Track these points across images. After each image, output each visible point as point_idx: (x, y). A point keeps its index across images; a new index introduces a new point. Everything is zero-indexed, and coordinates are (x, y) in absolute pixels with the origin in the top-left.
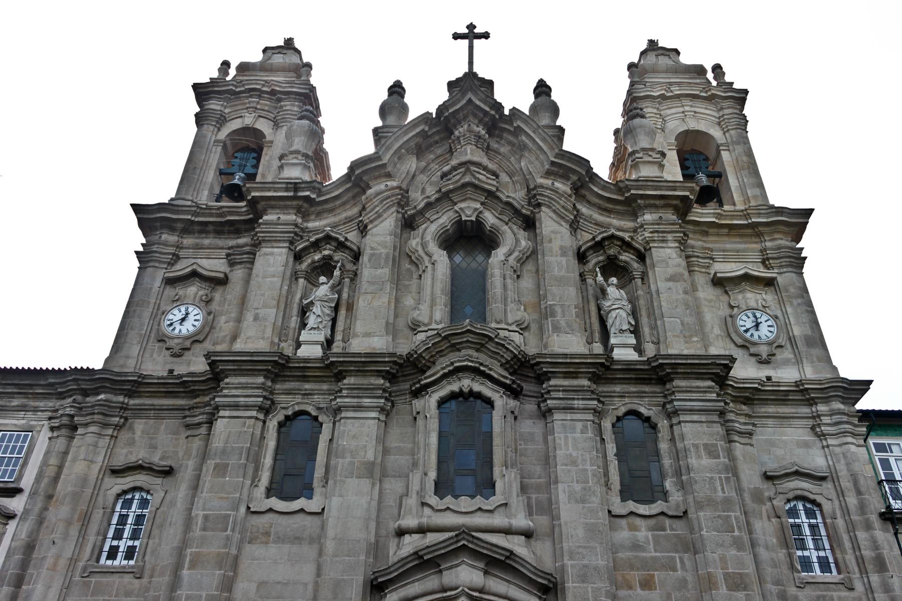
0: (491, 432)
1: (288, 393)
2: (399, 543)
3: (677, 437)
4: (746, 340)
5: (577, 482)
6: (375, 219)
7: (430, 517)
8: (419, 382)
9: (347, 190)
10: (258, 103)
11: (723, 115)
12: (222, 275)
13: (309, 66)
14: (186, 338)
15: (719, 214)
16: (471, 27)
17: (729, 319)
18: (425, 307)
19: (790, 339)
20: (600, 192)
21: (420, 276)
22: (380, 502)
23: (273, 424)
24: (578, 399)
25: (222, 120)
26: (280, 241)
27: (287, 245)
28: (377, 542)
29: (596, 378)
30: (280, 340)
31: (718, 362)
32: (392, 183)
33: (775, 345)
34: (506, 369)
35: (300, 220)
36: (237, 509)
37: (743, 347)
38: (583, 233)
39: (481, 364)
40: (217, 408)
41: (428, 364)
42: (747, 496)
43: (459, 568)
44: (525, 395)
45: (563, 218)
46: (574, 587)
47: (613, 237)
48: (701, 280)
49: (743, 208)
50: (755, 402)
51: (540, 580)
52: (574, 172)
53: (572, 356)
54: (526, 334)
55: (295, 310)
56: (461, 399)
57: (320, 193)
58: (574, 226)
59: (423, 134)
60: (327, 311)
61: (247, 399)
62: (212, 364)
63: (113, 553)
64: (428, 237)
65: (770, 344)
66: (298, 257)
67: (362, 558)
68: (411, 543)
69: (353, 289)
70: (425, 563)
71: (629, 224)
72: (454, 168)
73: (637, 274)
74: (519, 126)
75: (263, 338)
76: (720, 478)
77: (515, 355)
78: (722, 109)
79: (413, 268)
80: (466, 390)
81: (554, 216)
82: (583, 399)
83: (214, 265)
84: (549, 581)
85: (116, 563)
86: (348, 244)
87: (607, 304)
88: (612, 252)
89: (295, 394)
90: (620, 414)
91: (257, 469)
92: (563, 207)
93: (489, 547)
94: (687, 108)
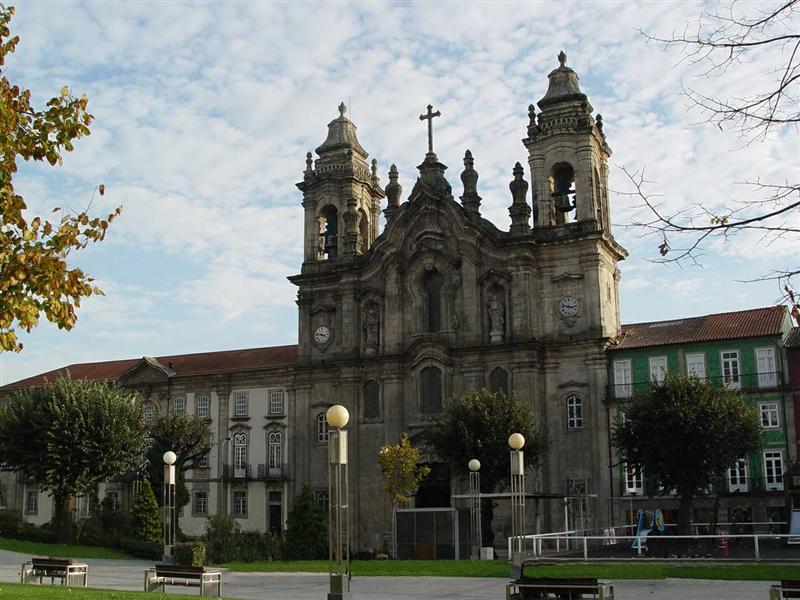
23: (361, 387)
25: (315, 203)
32: (393, 250)
48: (546, 280)
58: (479, 264)
65: (574, 316)
83: (329, 301)
94: (558, 144)
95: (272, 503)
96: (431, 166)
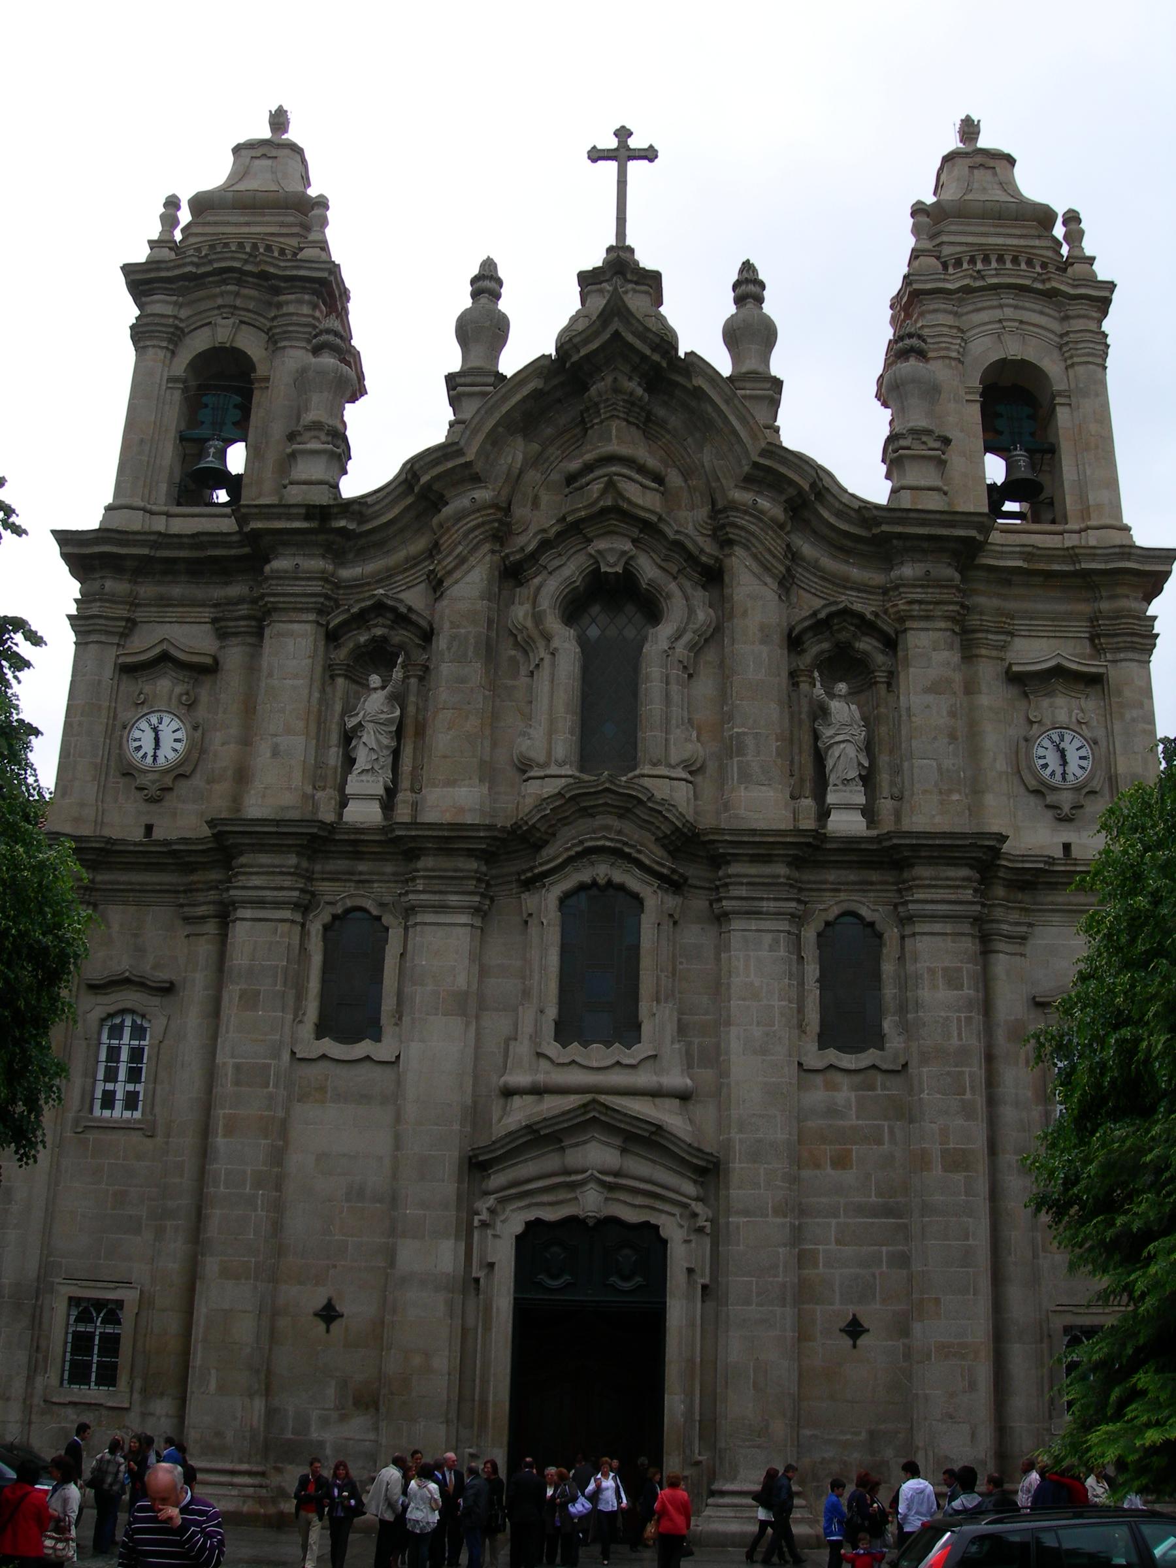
0: (636, 947)
1: (333, 878)
2: (504, 1109)
3: (907, 955)
4: (1043, 783)
5: (758, 1024)
6: (456, 568)
7: (548, 1073)
8: (531, 869)
9: (407, 509)
10: (237, 294)
11: (1067, 333)
12: (208, 661)
13: (322, 203)
14: (167, 772)
15: (1029, 553)
16: (623, 134)
17: (1023, 744)
19: (1110, 779)
20: (832, 520)
21: (532, 672)
22: (477, 1047)
23: (315, 928)
24: (768, 899)
25: (176, 336)
26: (301, 610)
27: (312, 617)
28: (475, 1103)
29: (797, 863)
30: (314, 788)
31: (980, 843)
32: (483, 495)
34: (663, 846)
35: (330, 568)
36: (277, 1056)
37: (1037, 792)
38: (801, 592)
39: (626, 844)
40: (234, 904)
41: (545, 837)
42: (1001, 1035)
43: (588, 1146)
44: (690, 886)
45: (767, 569)
46: (742, 1169)
47: (846, 612)
48: (988, 671)
49: (1076, 527)
50: (1040, 887)
51: (695, 1161)
52: (791, 482)
53: (764, 833)
54: (699, 779)
55: (334, 738)
56: (594, 892)
57: (362, 518)
58: (786, 584)
59: (536, 395)
60: (385, 741)
61: (275, 893)
62: (218, 837)
63: (108, 1100)
64: (545, 603)
65: (1077, 789)
66: (332, 637)
67: (456, 1127)
68: (521, 1112)
70: (541, 1137)
71: (876, 578)
72: (588, 468)
73: (881, 676)
74: (700, 388)
75: (289, 789)
76: (959, 1019)
77: (677, 828)
78: (1066, 318)
79: (519, 656)
80: (601, 881)
81: (755, 566)
82: (775, 899)
83: (192, 637)
84: (708, 1161)
85: (117, 1113)
86: (414, 617)
87: (828, 732)
88: (843, 636)
89: (345, 881)
90: (831, 917)
91: (300, 997)
92: (769, 551)
93: (628, 1120)
94: (1009, 312)
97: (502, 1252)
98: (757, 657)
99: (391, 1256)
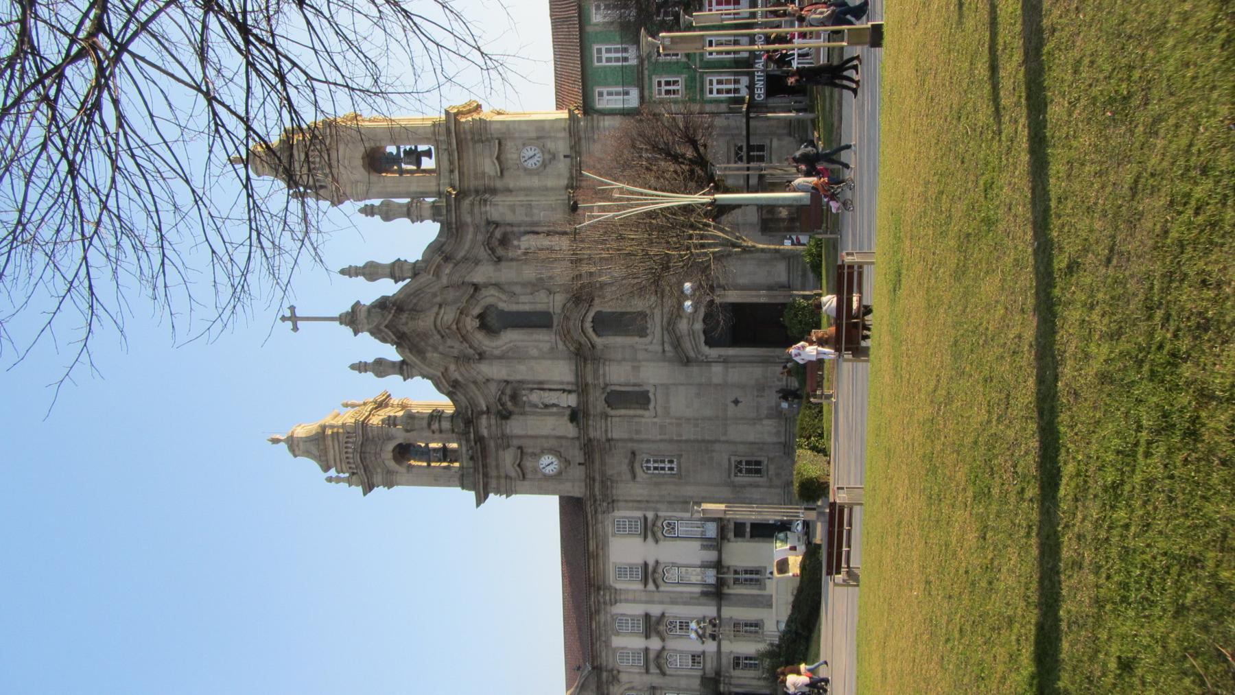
1: (595, 407)
18: (541, 345)
23: (613, 412)
25: (389, 472)
32: (452, 367)
33: (543, 149)
58: (477, 262)
63: (671, 469)
64: (494, 344)
65: (543, 153)
68: (668, 347)
69: (529, 382)
71: (471, 229)
95: (748, 535)
96: (352, 319)
97: (714, 352)
98: (506, 273)
99: (717, 385)
